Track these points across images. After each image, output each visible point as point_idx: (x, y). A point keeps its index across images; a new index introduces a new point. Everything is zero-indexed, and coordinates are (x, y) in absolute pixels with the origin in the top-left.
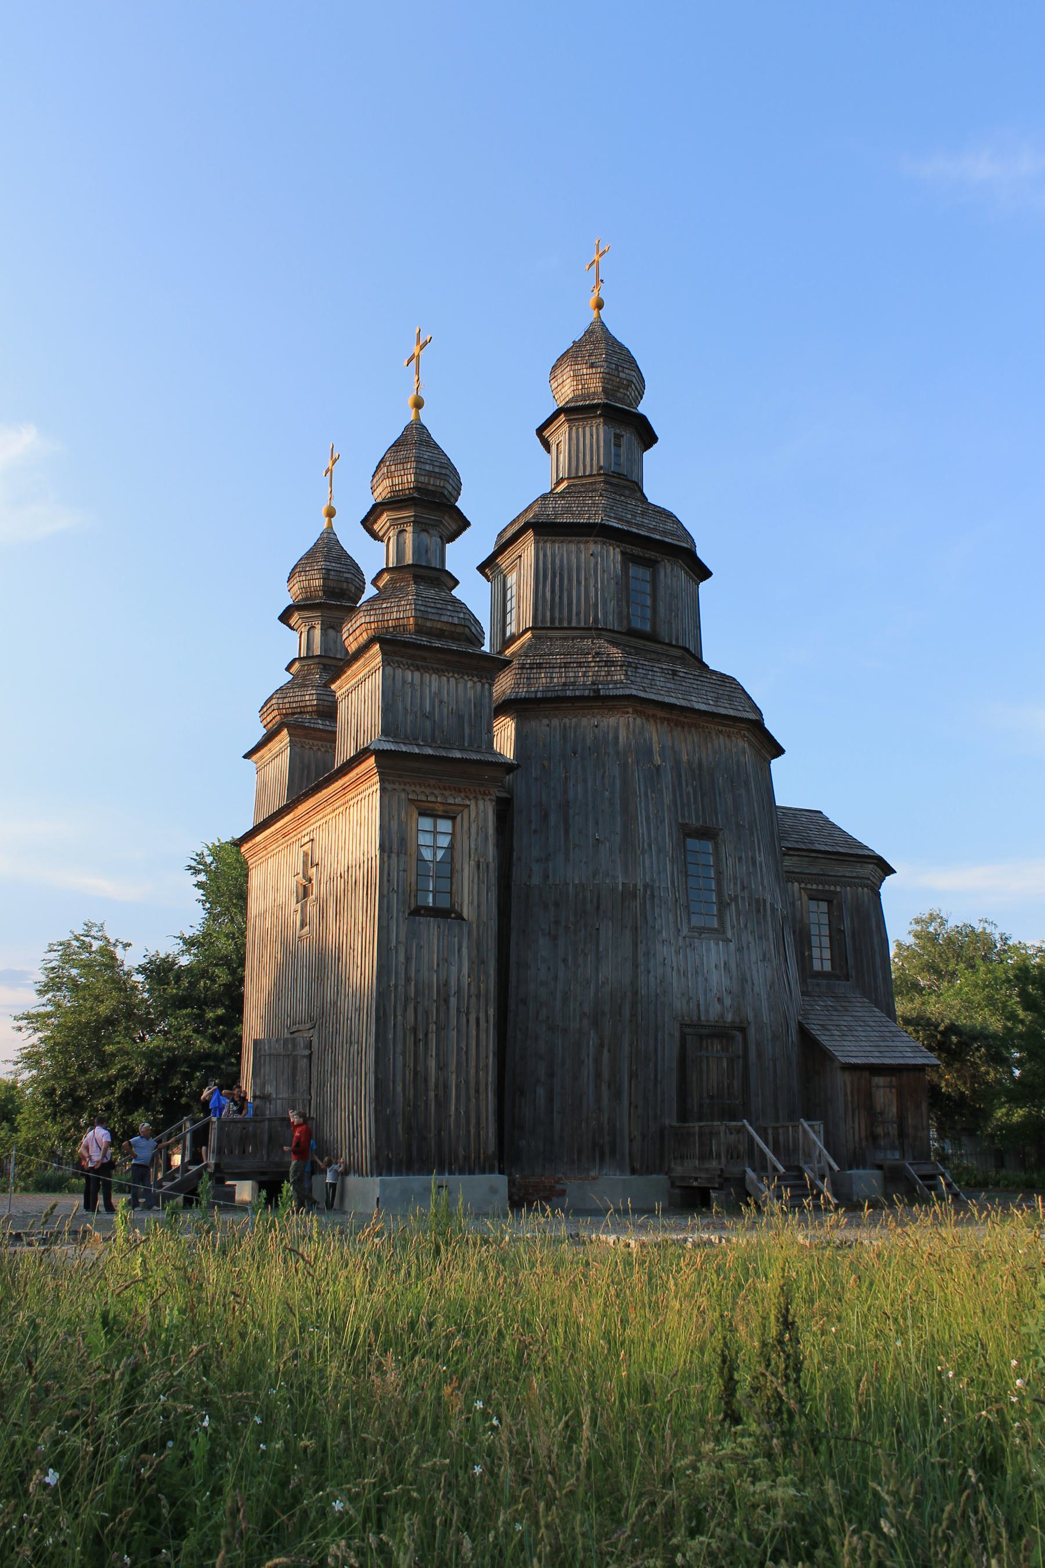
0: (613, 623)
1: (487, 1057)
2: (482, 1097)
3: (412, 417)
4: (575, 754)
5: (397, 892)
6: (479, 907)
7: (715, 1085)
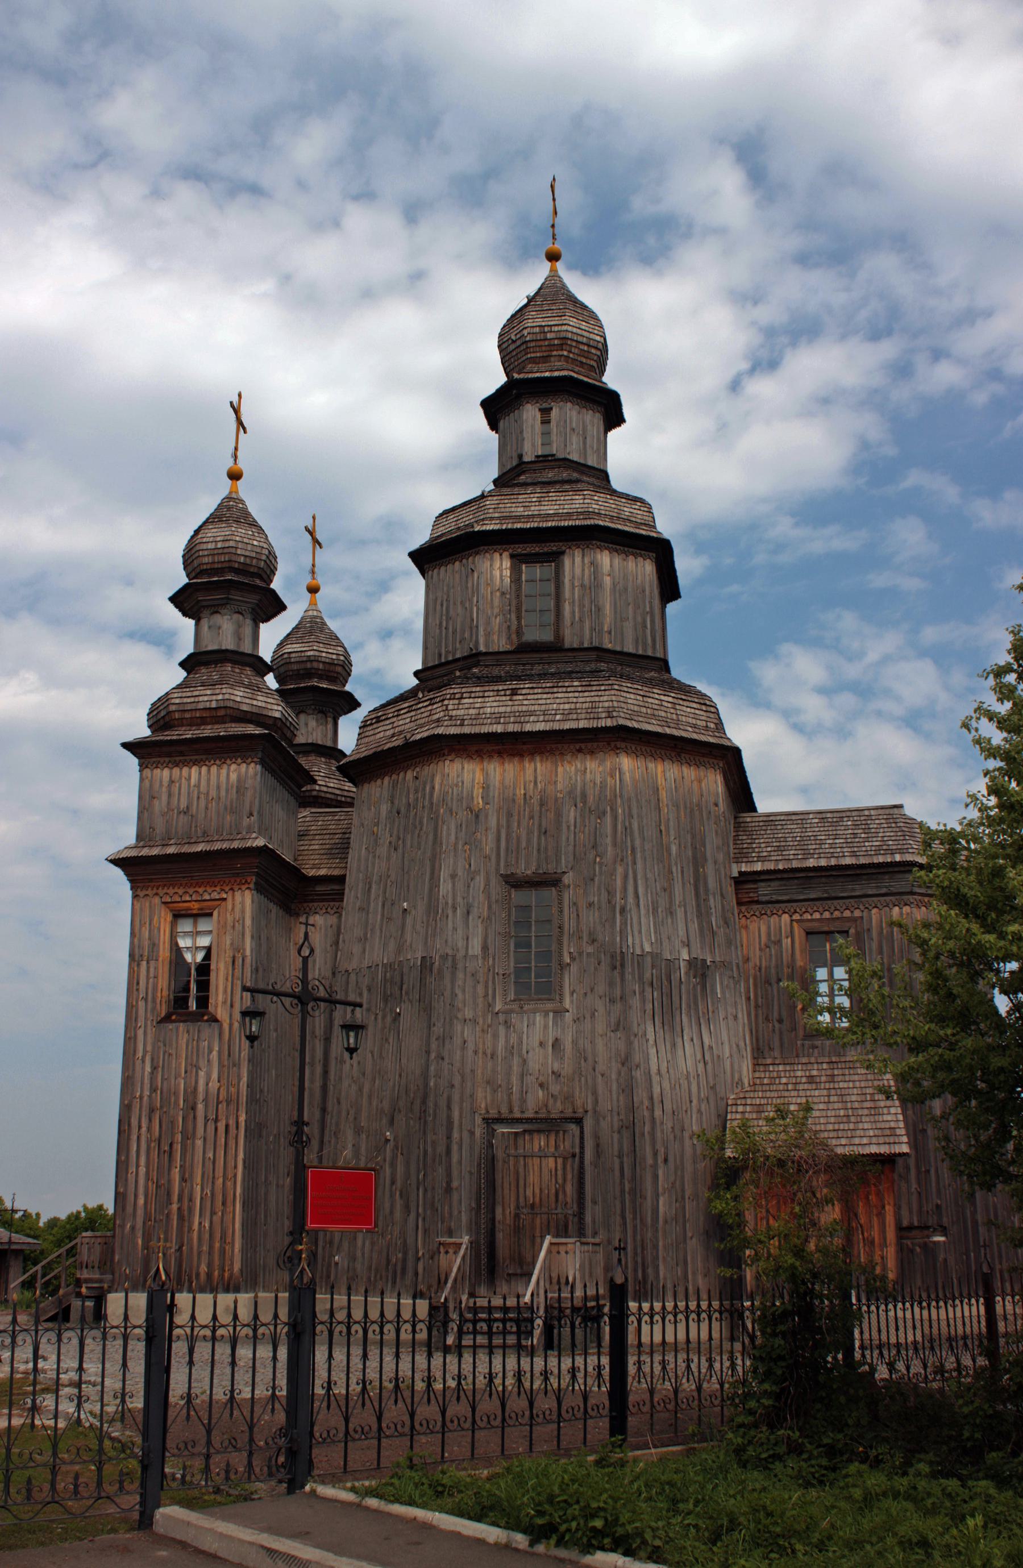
0: (501, 643)
1: (236, 1167)
2: (230, 1209)
3: (225, 493)
4: (398, 813)
5: (145, 999)
6: (232, 1006)
7: (537, 1191)
